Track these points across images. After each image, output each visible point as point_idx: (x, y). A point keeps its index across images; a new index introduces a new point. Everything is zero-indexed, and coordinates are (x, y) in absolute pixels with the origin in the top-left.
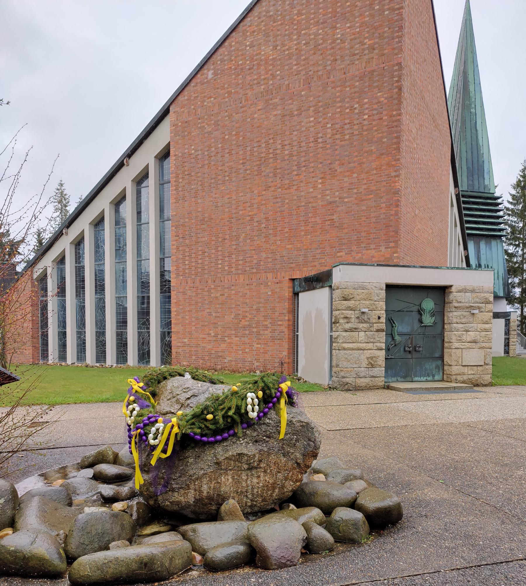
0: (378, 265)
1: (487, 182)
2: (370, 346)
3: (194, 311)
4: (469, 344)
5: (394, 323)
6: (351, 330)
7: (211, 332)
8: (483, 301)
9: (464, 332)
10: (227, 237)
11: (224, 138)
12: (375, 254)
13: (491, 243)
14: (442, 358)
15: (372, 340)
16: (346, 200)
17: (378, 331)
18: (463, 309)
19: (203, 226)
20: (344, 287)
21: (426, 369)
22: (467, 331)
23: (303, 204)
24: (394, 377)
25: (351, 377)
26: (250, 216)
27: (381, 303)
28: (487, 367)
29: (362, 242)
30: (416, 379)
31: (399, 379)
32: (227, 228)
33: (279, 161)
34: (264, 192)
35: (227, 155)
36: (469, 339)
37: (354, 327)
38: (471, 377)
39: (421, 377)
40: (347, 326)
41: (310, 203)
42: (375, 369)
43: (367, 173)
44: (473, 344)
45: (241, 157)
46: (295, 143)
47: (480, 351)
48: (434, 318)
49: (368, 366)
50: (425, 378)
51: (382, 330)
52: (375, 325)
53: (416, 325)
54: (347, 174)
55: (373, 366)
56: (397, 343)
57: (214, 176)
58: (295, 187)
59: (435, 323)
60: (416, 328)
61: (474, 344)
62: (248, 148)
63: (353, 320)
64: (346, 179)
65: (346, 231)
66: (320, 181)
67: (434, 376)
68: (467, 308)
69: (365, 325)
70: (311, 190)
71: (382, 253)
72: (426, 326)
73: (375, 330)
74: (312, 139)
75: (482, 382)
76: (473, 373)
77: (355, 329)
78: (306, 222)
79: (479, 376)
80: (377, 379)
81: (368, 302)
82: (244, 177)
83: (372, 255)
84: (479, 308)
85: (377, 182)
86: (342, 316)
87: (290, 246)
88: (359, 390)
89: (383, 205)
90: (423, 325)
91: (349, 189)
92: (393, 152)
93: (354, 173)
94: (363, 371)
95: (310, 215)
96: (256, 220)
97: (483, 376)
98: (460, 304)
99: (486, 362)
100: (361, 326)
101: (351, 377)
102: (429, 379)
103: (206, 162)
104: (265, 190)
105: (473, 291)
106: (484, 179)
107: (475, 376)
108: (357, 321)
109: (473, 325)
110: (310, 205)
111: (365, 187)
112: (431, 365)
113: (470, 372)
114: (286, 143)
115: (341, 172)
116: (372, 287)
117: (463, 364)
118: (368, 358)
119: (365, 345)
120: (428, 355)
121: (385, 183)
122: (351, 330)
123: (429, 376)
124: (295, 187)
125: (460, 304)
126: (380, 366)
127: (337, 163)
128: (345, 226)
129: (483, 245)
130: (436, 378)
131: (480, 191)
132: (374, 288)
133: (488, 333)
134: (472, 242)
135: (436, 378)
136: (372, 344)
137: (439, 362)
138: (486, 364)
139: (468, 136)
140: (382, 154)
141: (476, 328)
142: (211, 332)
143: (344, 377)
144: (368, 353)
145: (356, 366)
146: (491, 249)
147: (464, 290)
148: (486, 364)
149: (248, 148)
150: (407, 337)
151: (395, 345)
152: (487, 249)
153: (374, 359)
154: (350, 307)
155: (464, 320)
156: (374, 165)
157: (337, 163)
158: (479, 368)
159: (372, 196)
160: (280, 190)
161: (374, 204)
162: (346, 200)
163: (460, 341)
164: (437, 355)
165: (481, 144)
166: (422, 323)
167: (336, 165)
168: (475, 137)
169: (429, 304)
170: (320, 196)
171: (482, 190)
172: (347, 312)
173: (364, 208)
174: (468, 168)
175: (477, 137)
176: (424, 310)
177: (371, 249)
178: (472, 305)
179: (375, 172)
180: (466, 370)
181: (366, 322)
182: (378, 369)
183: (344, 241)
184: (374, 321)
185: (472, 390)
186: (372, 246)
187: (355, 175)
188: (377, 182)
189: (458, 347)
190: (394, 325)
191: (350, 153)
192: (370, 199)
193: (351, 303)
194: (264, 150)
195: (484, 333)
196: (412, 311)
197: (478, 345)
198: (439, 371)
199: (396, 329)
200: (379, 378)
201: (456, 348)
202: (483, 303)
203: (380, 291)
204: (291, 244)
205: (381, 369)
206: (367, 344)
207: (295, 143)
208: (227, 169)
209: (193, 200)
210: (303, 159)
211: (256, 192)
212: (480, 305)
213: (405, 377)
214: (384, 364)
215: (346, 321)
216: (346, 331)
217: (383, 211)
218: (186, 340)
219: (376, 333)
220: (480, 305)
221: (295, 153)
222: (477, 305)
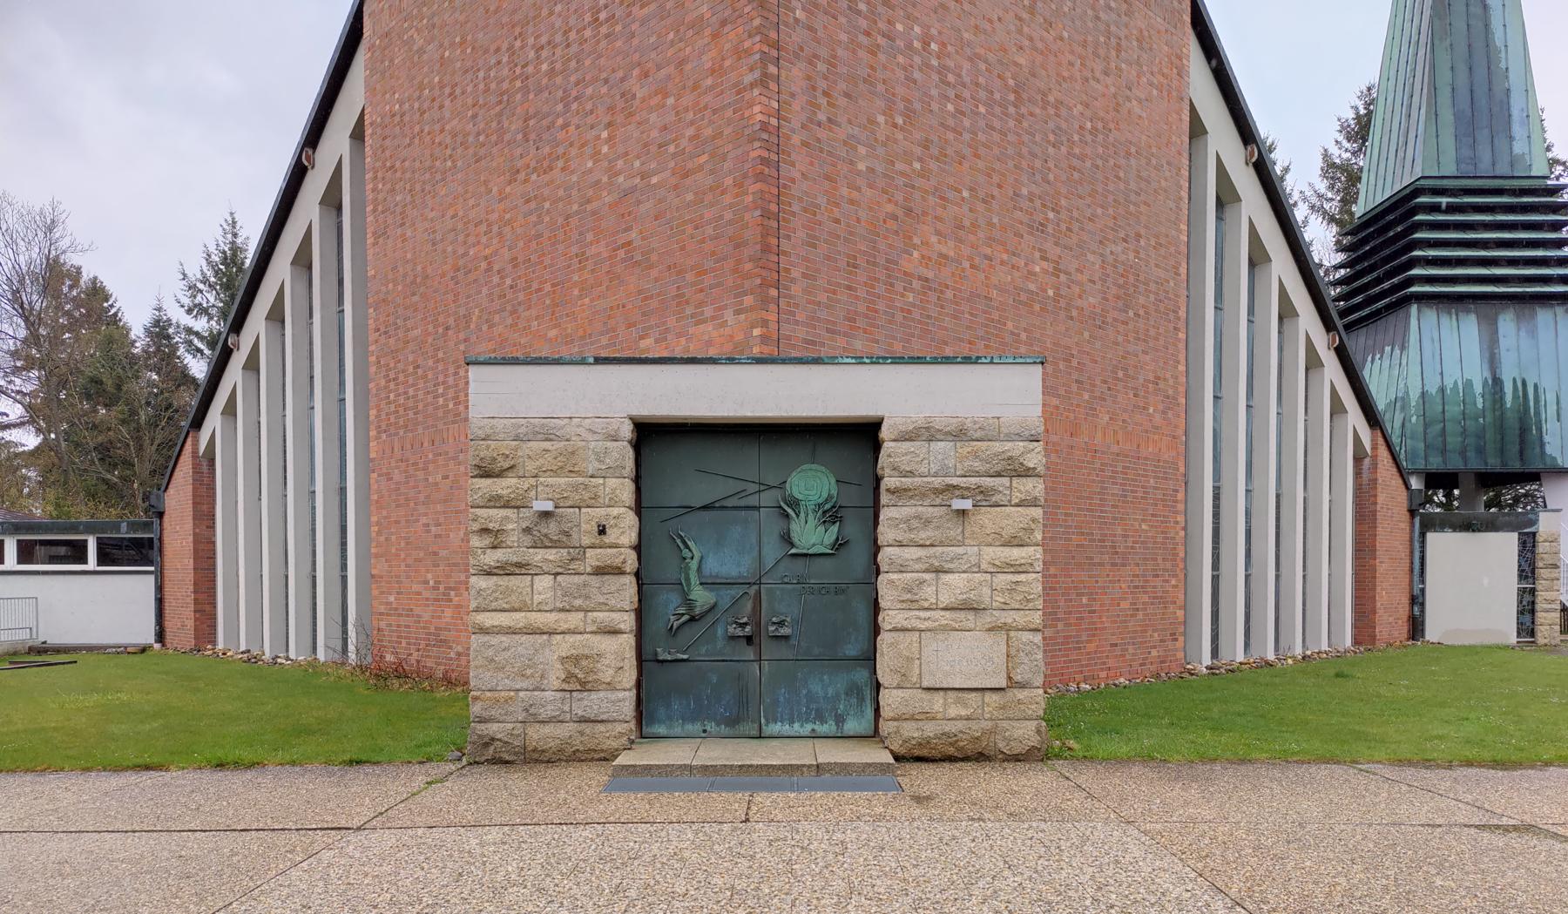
0: (599, 361)
1: (1518, 148)
2: (574, 619)
3: (403, 523)
4: (947, 614)
5: (687, 547)
6: (504, 570)
7: (429, 576)
8: (999, 468)
9: (927, 576)
10: (451, 321)
11: (442, 57)
12: (715, 334)
13: (1533, 316)
14: (869, 658)
15: (578, 602)
16: (654, 180)
17: (600, 571)
18: (923, 496)
19: (416, 298)
20: (481, 433)
21: (811, 697)
22: (938, 571)
23: (575, 207)
24: (693, 720)
25: (508, 718)
26: (486, 258)
27: (612, 482)
28: (1021, 694)
29: (687, 302)
30: (776, 728)
32: (450, 297)
33: (531, 96)
34: (508, 189)
35: (447, 103)
36: (945, 599)
37: (515, 559)
38: (950, 727)
39: (792, 722)
40: (492, 558)
41: (589, 201)
42: (594, 696)
43: (695, 88)
44: (962, 615)
45: (470, 101)
46: (558, 38)
47: (989, 639)
48: (835, 529)
49: (566, 687)
50: (809, 727)
51: (619, 571)
52: (590, 553)
54: (656, 100)
55: (585, 687)
56: (697, 611)
57: (428, 164)
58: (560, 164)
59: (839, 545)
61: (971, 615)
62: (481, 74)
63: (512, 539)
64: (653, 117)
65: (654, 273)
66: (605, 135)
67: (840, 720)
68: (937, 492)
69: (552, 554)
70: (590, 164)
71: (728, 331)
72: (805, 555)
73: (589, 569)
74: (588, 18)
75: (1001, 745)
76: (963, 713)
77: (519, 565)
78: (582, 258)
79: (988, 725)
80: (601, 727)
81: (563, 480)
82: (475, 154)
83: (706, 338)
84: (983, 491)
85: (715, 112)
86: (476, 526)
87: (552, 333)
88: (536, 761)
89: (729, 181)
90: (793, 551)
91: (660, 146)
92: (746, 10)
93: (666, 96)
94: (550, 701)
95: (590, 237)
96: (496, 267)
97: (1005, 724)
98: (907, 481)
99: (1018, 678)
100: (538, 556)
101: (508, 718)
102: (823, 729)
103: (417, 129)
104: (510, 183)
105: (959, 434)
106: (1511, 138)
107: (971, 724)
108: (527, 540)
109: (960, 550)
110: (589, 208)
111: (690, 132)
112: (826, 685)
113: (953, 711)
114: (544, 40)
115: (643, 100)
116: (579, 430)
117: (925, 684)
118: (563, 660)
119: (553, 617)
120: (816, 651)
121: (729, 113)
122: (504, 570)
123: (823, 721)
124: (560, 164)
125: (907, 481)
126: (611, 687)
127: (636, 72)
128: (654, 257)
129: (1507, 322)
130: (851, 726)
131: (1498, 173)
132: (590, 437)
133: (1022, 577)
134: (1473, 318)
135: (851, 726)
136: (581, 615)
137: (861, 675)
138: (1013, 684)
139: (1460, 25)
140: (724, 23)
141: (974, 560)
142: (429, 576)
143: (483, 721)
144: (564, 646)
145: (524, 685)
146: (1533, 333)
147: (925, 433)
148: (1013, 684)
149: (481, 74)
150: (736, 592)
151: (692, 619)
152: (1523, 334)
153: (584, 663)
154: (499, 497)
155: (923, 535)
156: (707, 61)
157: (636, 72)
158: (989, 697)
159: (705, 158)
160: (534, 177)
161: (709, 180)
162: (654, 180)
163: (912, 604)
164: (852, 650)
165: (1499, 42)
166: (792, 545)
167: (633, 84)
168: (1481, 25)
169: (812, 483)
170: (605, 179)
171: (1503, 169)
172: (492, 512)
173: (690, 197)
174: (1457, 116)
175: (1487, 26)
176: (794, 503)
177: (704, 321)
178: (955, 481)
179: (709, 82)
180: (937, 703)
181: (556, 545)
182: (602, 694)
183: (654, 303)
184: (586, 541)
185: (887, 778)
186: (708, 311)
187: (671, 101)
188: (715, 112)
189: (906, 624)
190: (686, 553)
191: (659, 36)
192: (700, 168)
193: (503, 486)
194: (505, 72)
195: (1002, 579)
196: (757, 508)
197: (987, 619)
198: (861, 700)
199: (694, 565)
200: (610, 726)
201: (895, 630)
202: (999, 475)
203: (609, 444)
204: (555, 326)
205: (621, 695)
206: (562, 615)
207: (558, 38)
208: (448, 140)
209: (399, 231)
210: (573, 79)
211: (495, 189)
212: (988, 482)
213: (733, 722)
214: (629, 676)
215: (487, 541)
216: (489, 574)
217: (728, 199)
218: (392, 599)
219: (595, 581)
220: (988, 482)
221: (558, 66)
222: (973, 480)
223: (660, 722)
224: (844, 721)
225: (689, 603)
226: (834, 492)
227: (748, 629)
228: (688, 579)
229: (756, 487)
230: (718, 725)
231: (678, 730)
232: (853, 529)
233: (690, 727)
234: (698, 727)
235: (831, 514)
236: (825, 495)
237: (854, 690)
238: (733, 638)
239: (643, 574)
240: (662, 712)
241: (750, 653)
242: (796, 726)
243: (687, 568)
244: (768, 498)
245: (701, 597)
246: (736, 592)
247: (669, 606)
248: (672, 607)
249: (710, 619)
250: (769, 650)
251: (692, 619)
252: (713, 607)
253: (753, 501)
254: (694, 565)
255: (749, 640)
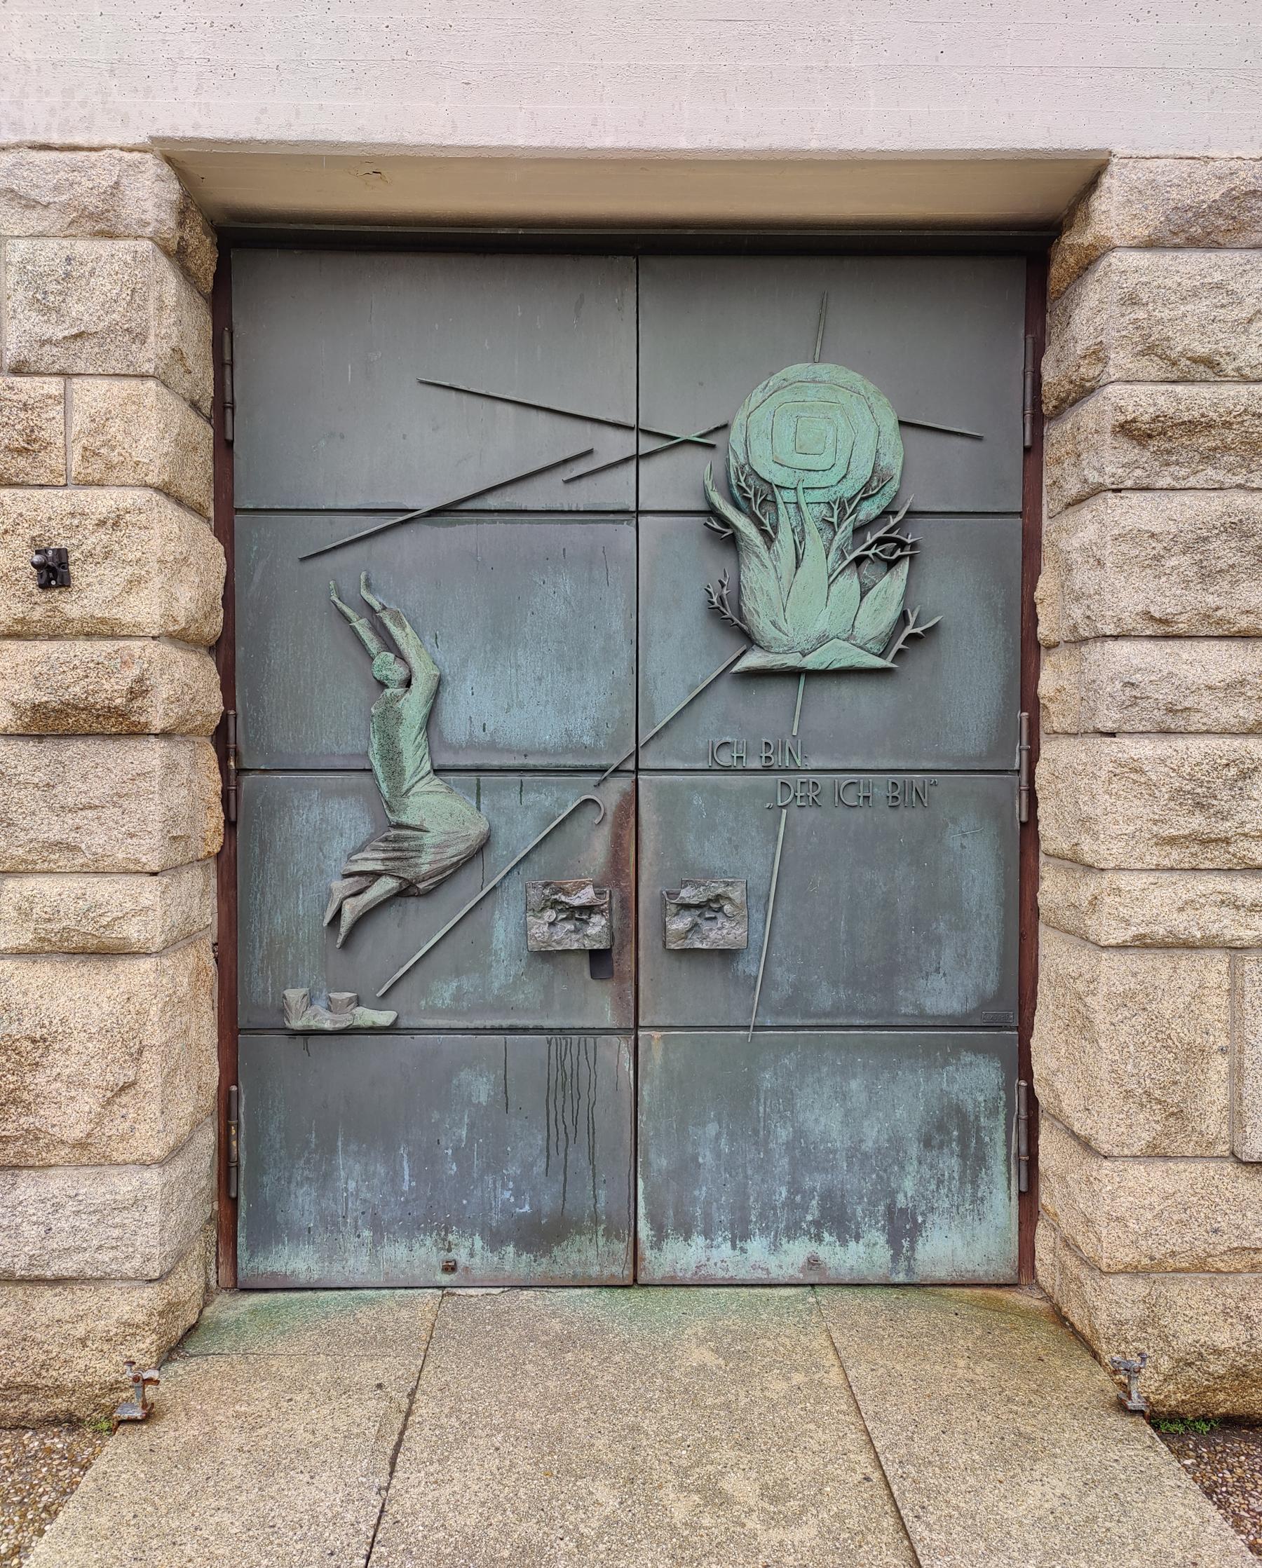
5: (390, 644)
14: (1008, 1019)
21: (805, 1155)
24: (413, 1228)
30: (683, 1255)
31: (470, 1251)
39: (740, 1235)
48: (893, 584)
50: (797, 1252)
53: (681, 658)
56: (426, 863)
59: (911, 639)
60: (667, 698)
67: (903, 1228)
72: (794, 674)
90: (754, 660)
102: (847, 1258)
112: (850, 1111)
120: (825, 997)
135: (944, 1248)
137: (977, 1080)
150: (559, 798)
151: (407, 891)
164: (948, 990)
166: (749, 639)
176: (757, 497)
198: (974, 1162)
223: (302, 1235)
224: (915, 1231)
225: (398, 837)
226: (893, 461)
227: (597, 925)
228: (392, 755)
229: (622, 445)
230: (495, 1240)
231: (357, 1265)
232: (952, 589)
233: (397, 1253)
234: (419, 1255)
235: (882, 540)
236: (862, 472)
237: (950, 1129)
238: (546, 956)
239: (241, 736)
240: (303, 1202)
241: (600, 1006)
242: (757, 1247)
243: (390, 718)
244: (672, 481)
245: (441, 816)
246: (559, 798)
247: (327, 847)
248: (339, 847)
249: (467, 890)
250: (669, 996)
251: (407, 891)
252: (483, 847)
253: (615, 490)
254: (413, 706)
255: (599, 960)
